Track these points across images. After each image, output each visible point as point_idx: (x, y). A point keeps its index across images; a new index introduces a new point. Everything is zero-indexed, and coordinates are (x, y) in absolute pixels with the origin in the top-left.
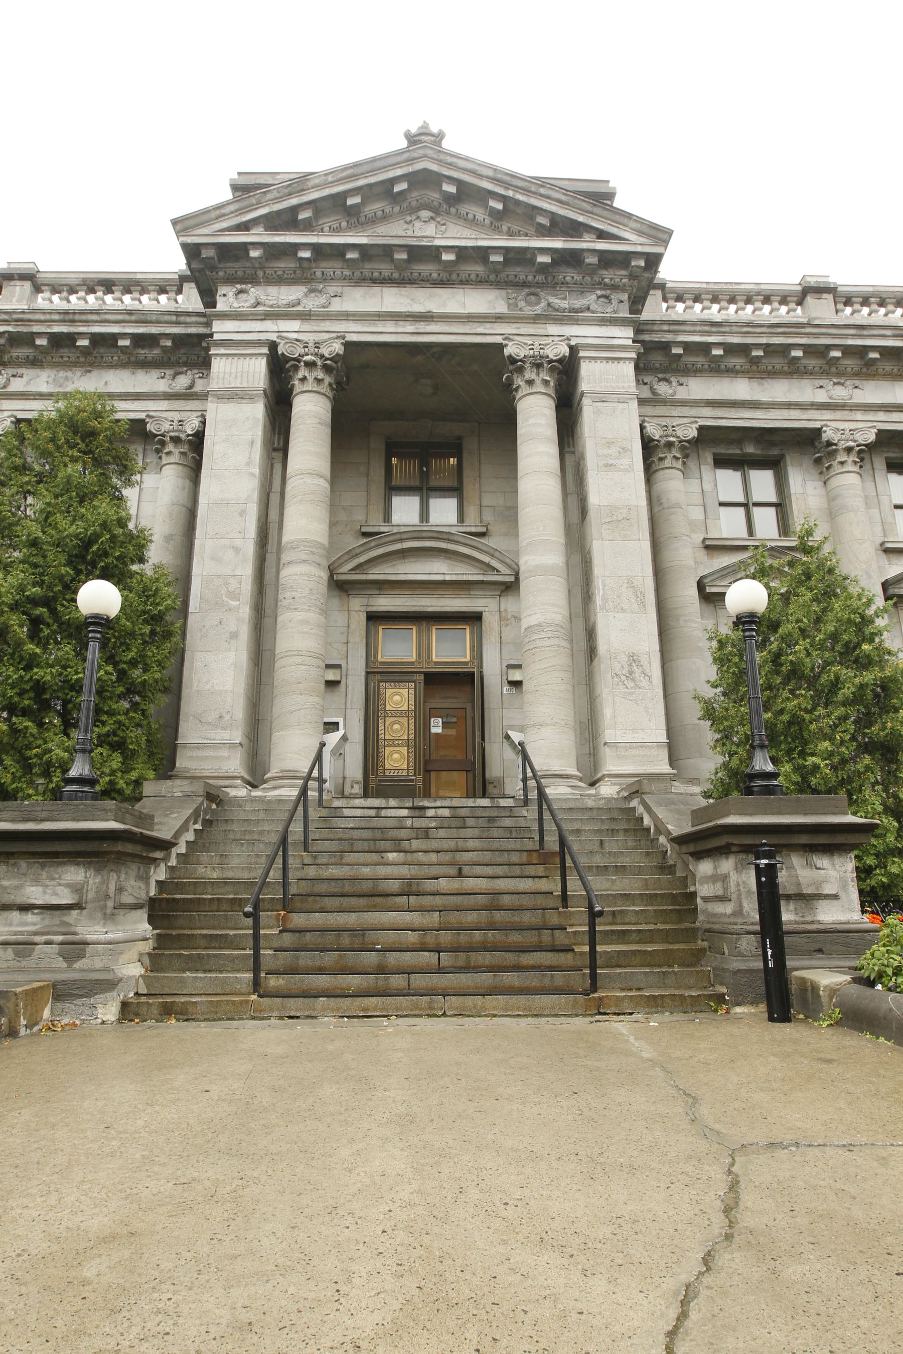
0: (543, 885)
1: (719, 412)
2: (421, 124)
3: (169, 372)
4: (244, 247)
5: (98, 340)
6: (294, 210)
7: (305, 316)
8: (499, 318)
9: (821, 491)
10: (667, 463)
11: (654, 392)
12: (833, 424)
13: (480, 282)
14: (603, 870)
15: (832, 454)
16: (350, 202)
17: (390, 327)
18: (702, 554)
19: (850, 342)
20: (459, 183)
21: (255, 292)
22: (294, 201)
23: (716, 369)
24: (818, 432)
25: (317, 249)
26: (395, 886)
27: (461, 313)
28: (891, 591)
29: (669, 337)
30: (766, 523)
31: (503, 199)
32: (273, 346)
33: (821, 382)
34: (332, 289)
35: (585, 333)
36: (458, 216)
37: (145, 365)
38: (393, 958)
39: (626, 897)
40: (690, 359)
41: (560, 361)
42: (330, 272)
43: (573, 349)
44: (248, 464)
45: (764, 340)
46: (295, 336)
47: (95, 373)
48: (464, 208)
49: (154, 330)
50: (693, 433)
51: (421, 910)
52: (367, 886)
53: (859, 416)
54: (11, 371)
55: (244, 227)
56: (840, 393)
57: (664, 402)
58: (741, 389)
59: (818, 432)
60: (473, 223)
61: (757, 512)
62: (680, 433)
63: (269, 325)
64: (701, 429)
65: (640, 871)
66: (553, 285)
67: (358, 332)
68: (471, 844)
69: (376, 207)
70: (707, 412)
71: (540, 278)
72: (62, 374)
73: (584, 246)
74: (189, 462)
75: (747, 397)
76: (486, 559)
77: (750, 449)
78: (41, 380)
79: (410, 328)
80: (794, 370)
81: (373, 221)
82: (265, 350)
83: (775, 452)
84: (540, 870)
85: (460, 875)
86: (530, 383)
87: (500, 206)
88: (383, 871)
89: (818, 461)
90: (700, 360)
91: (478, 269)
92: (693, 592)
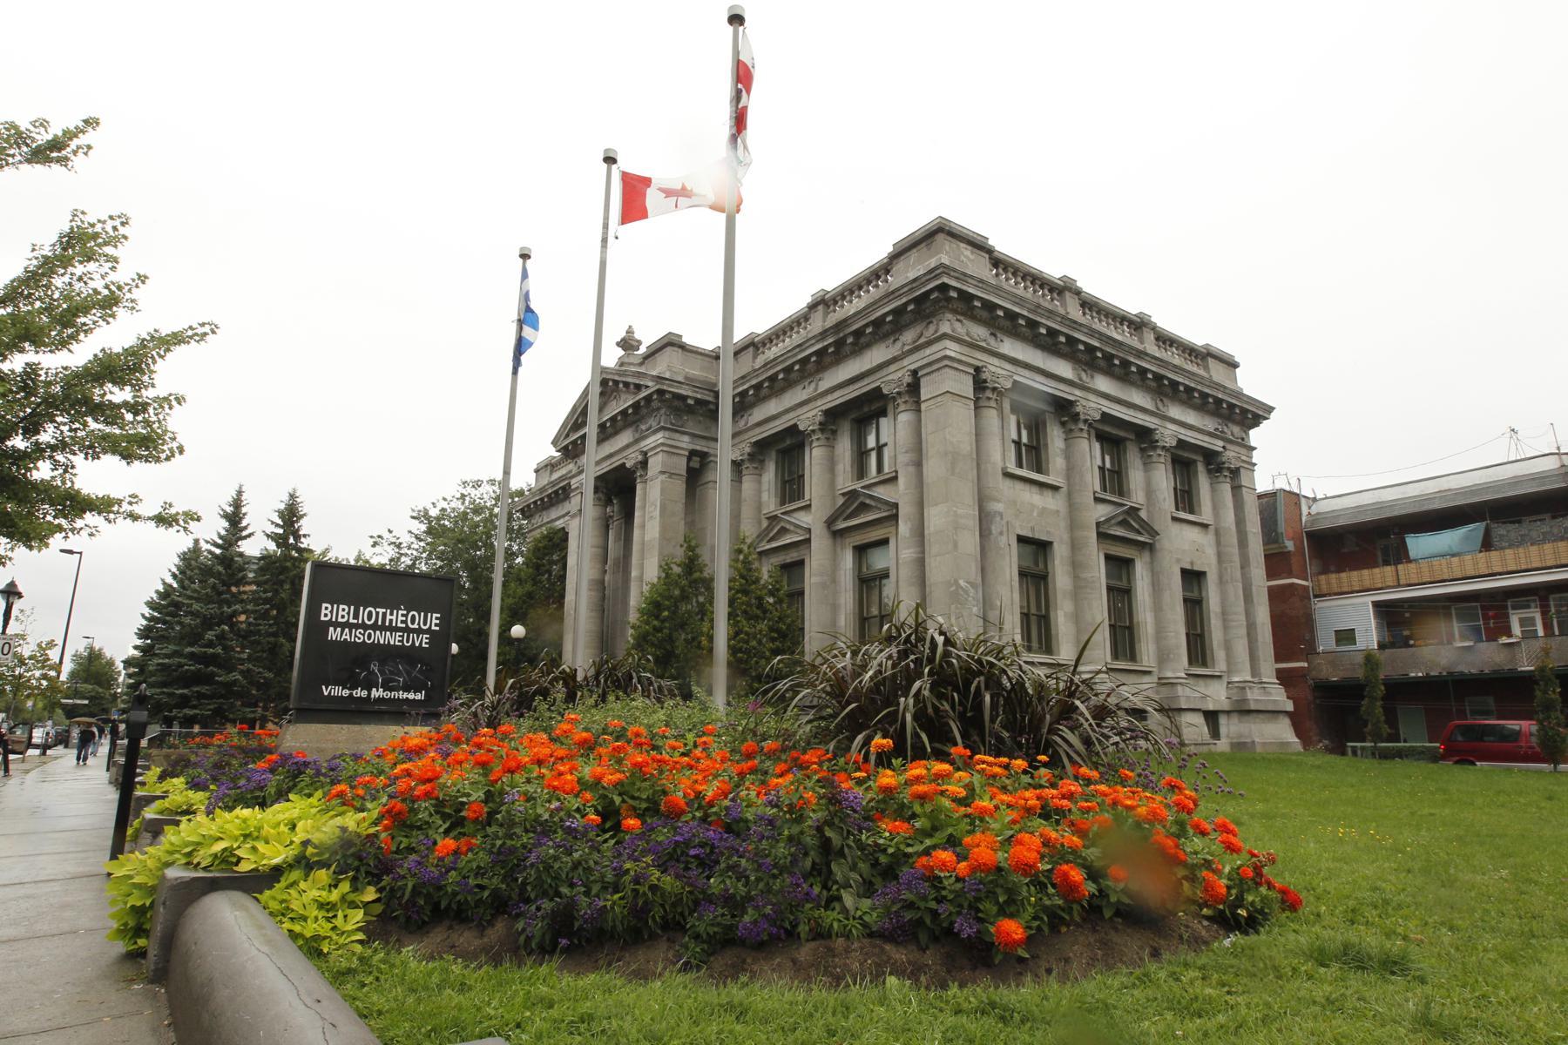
8: (627, 446)
59: (795, 425)
64: (756, 444)
66: (641, 419)
70: (758, 430)
80: (789, 384)
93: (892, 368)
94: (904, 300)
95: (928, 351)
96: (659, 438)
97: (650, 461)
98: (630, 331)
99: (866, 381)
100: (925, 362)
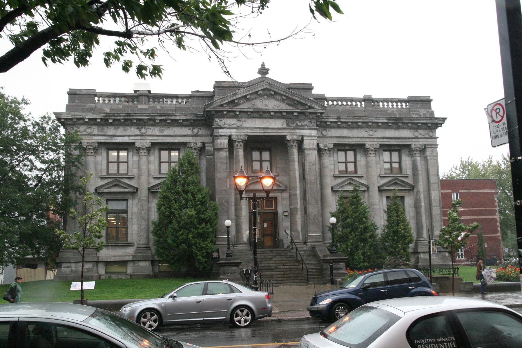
0: (299, 267)
1: (339, 140)
2: (261, 63)
3: (191, 128)
4: (222, 111)
5: (172, 120)
6: (234, 100)
7: (237, 128)
8: (284, 129)
9: (365, 160)
10: (325, 154)
11: (322, 134)
12: (369, 143)
13: (280, 118)
14: (308, 264)
15: (368, 151)
16: (248, 97)
17: (258, 131)
18: (333, 179)
19: (374, 121)
20: (275, 92)
21: (224, 120)
22: (234, 98)
23: (339, 127)
24: (364, 145)
25: (240, 112)
26: (273, 267)
27: (275, 126)
28: (381, 189)
29: (326, 120)
30: (351, 167)
31: (286, 96)
32: (230, 137)
33: (365, 130)
34: (243, 119)
35: (305, 132)
36: (274, 98)
37: (185, 126)
38: (278, 279)
39: (312, 269)
40: (333, 124)
41: (300, 141)
42: (243, 116)
43: (303, 137)
44: (227, 168)
45: (351, 121)
46: (235, 134)
47: (171, 128)
48: (275, 97)
49: (189, 118)
50: (332, 147)
51: (280, 271)
52: (269, 268)
53: (376, 140)
54: (147, 127)
55: (222, 106)
56: (371, 133)
57: (325, 137)
58: (345, 132)
59: (364, 145)
60: (278, 100)
61: (348, 164)
62: (328, 146)
63: (228, 130)
65: (314, 264)
67: (250, 132)
68: (284, 259)
69: (253, 96)
70: (336, 139)
71: (295, 117)
72: (161, 128)
73: (306, 111)
74: (199, 155)
75: (347, 136)
76: (279, 184)
77: (347, 148)
78: (156, 131)
79: (263, 131)
80: (359, 127)
81: (253, 99)
82: (228, 138)
83: (354, 148)
84: (297, 264)
85: (284, 265)
86: (292, 146)
87: (285, 98)
88: (270, 265)
89: (365, 151)
90: (334, 125)
91: (279, 115)
92: (330, 190)
93: (414, 140)
94: (429, 122)
95: (430, 140)
96: (314, 133)
97: (305, 142)
98: (263, 65)
99: (401, 140)
100: (428, 143)
